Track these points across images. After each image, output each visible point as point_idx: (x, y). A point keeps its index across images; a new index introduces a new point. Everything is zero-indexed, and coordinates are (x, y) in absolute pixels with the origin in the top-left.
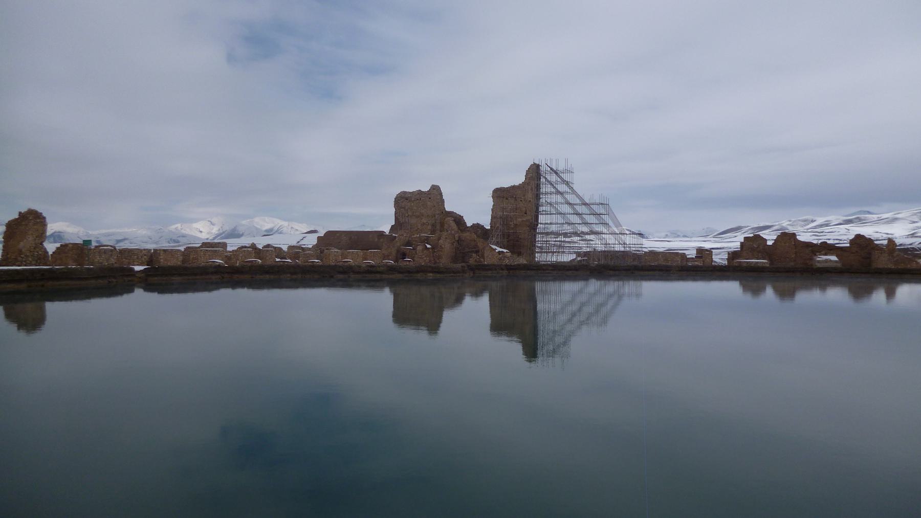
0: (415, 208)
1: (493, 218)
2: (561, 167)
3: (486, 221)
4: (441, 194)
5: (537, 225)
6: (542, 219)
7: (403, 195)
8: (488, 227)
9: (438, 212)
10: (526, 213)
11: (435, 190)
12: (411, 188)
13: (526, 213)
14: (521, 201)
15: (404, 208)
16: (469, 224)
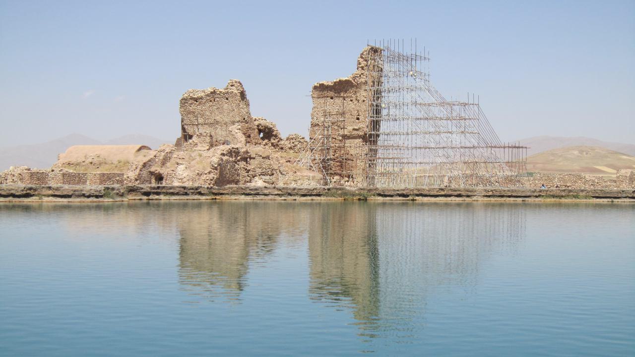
0: (208, 113)
1: (314, 125)
2: (408, 51)
3: (304, 132)
4: (243, 95)
5: (378, 136)
6: (384, 127)
7: (191, 95)
8: (308, 139)
9: (238, 119)
10: (358, 119)
11: (233, 87)
12: (203, 88)
13: (358, 119)
14: (351, 101)
15: (194, 113)
16: (283, 135)
